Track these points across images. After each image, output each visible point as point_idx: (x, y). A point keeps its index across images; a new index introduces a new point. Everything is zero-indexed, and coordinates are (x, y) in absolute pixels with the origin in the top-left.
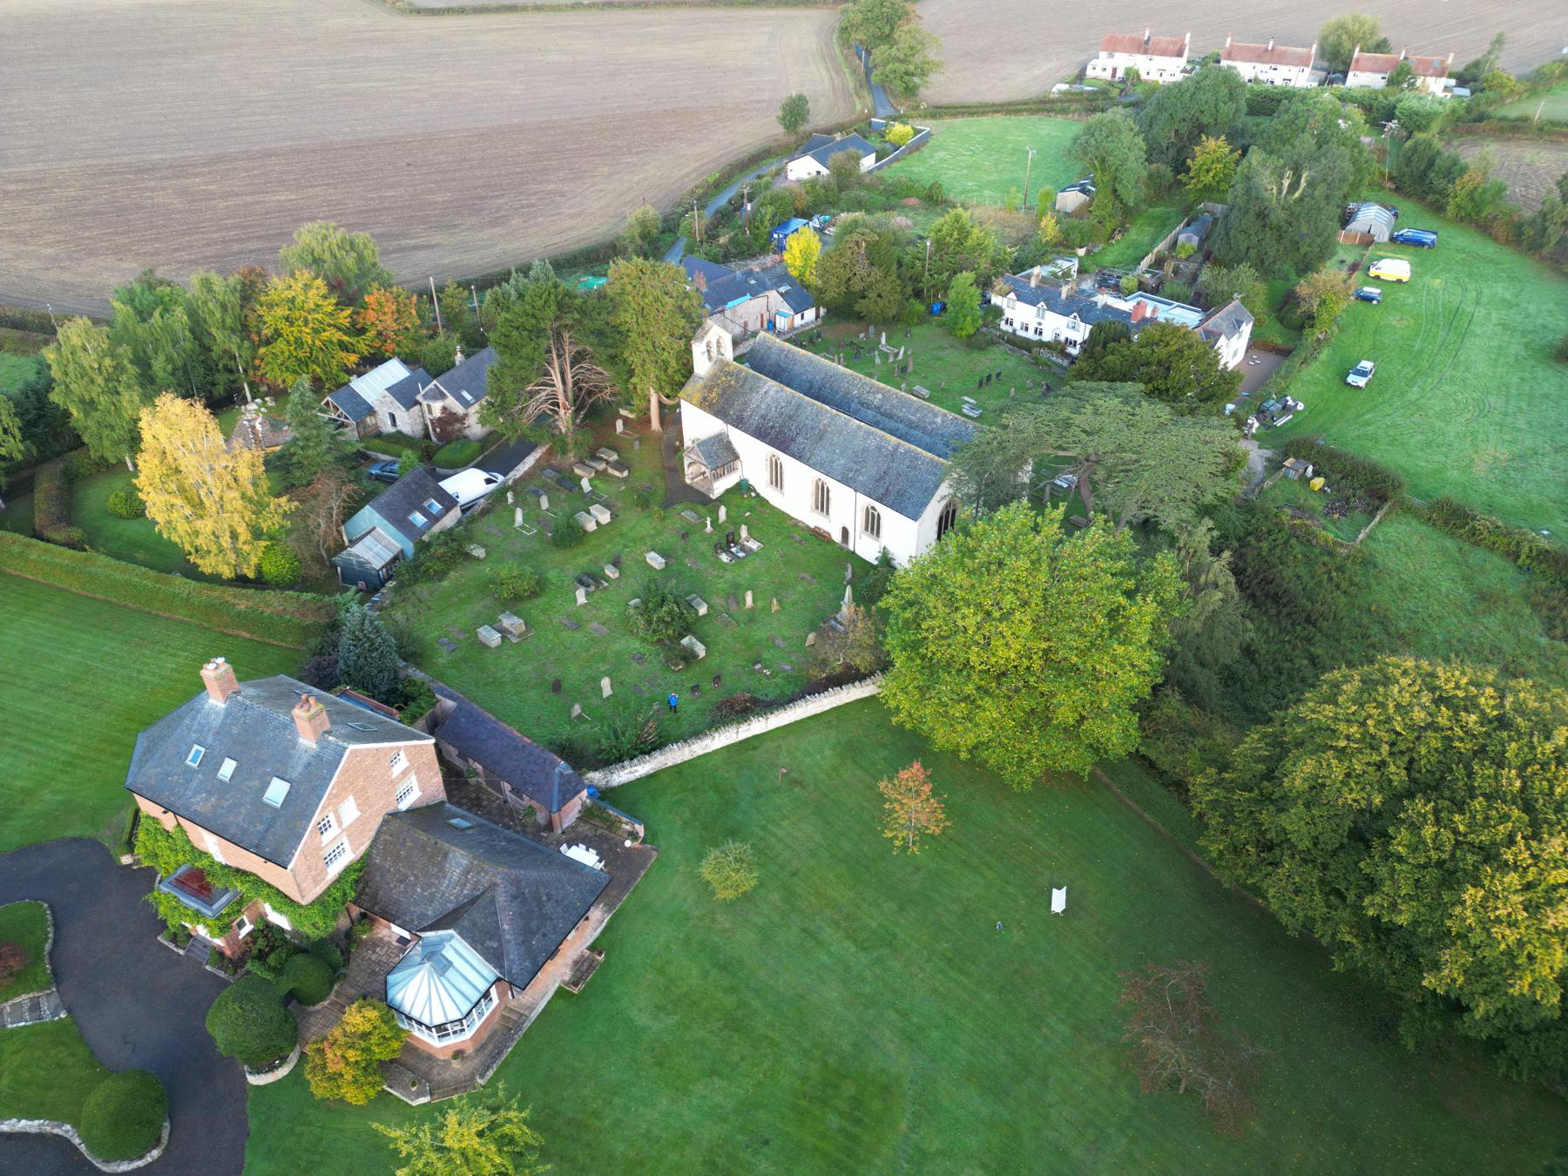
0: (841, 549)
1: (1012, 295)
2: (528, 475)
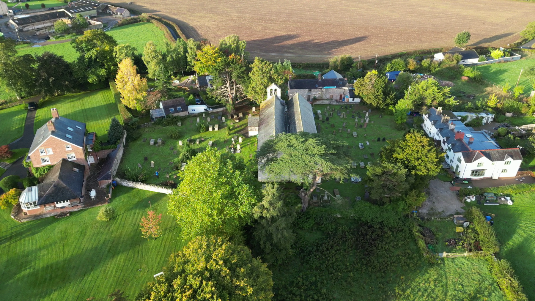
1: (427, 115)
2: (218, 112)
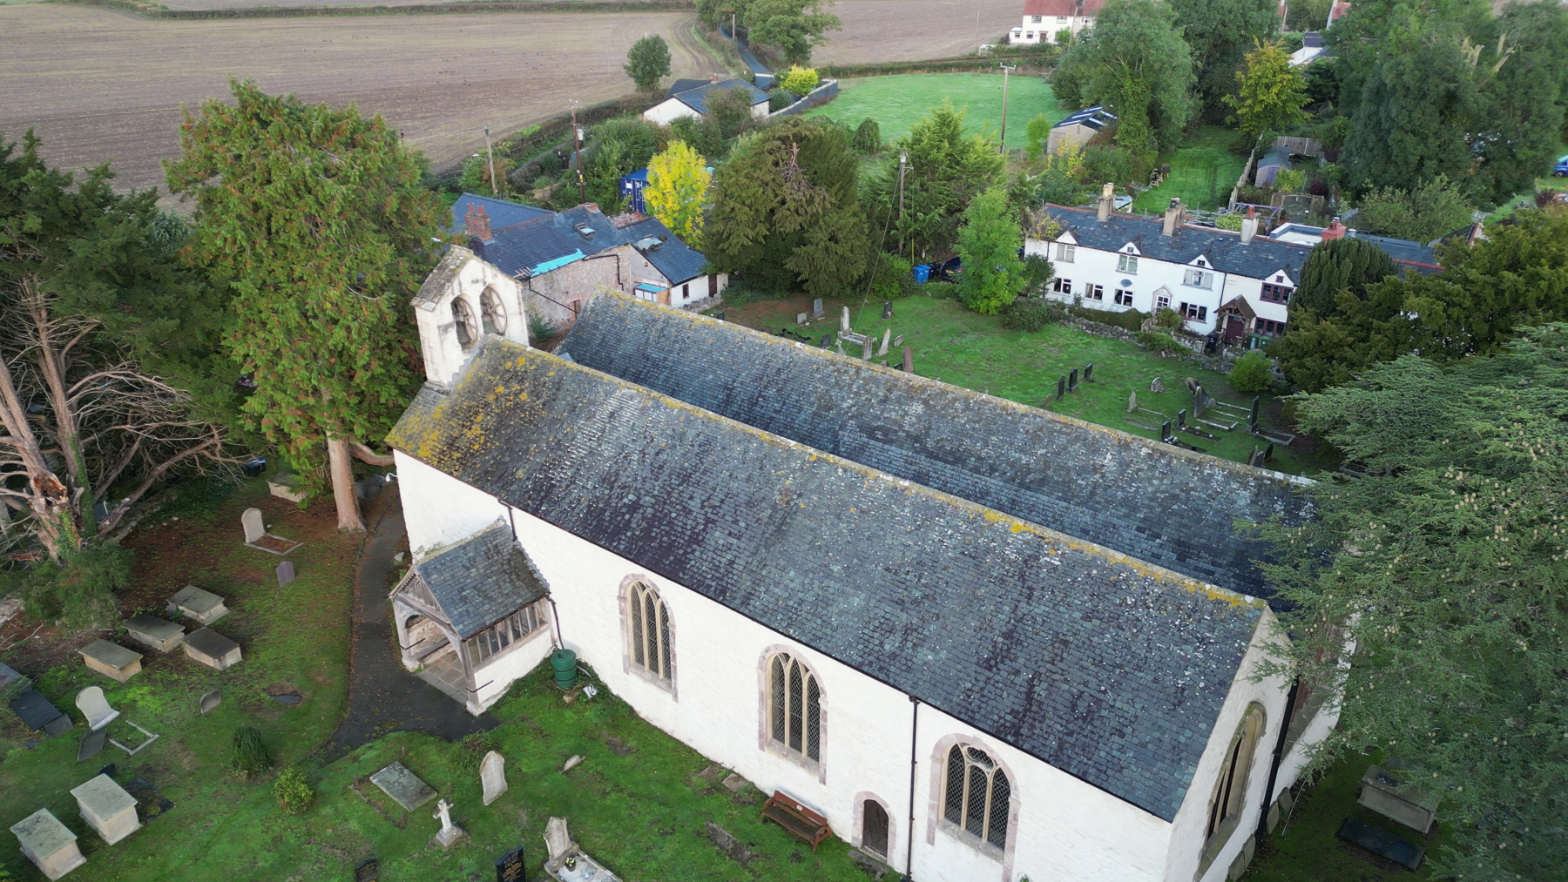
0: (867, 868)
1: (1067, 238)
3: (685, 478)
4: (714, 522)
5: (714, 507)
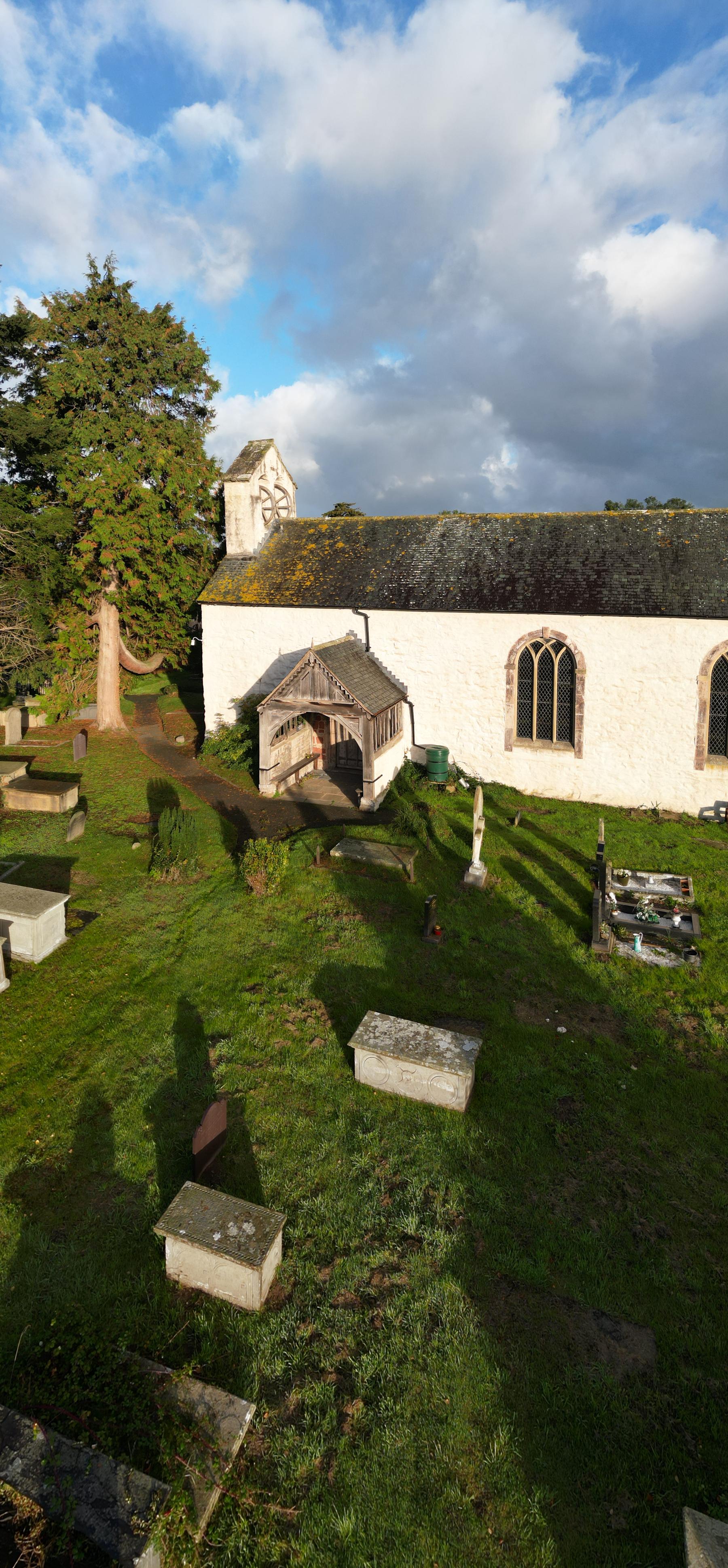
3: (552, 553)
4: (604, 571)
5: (598, 563)
